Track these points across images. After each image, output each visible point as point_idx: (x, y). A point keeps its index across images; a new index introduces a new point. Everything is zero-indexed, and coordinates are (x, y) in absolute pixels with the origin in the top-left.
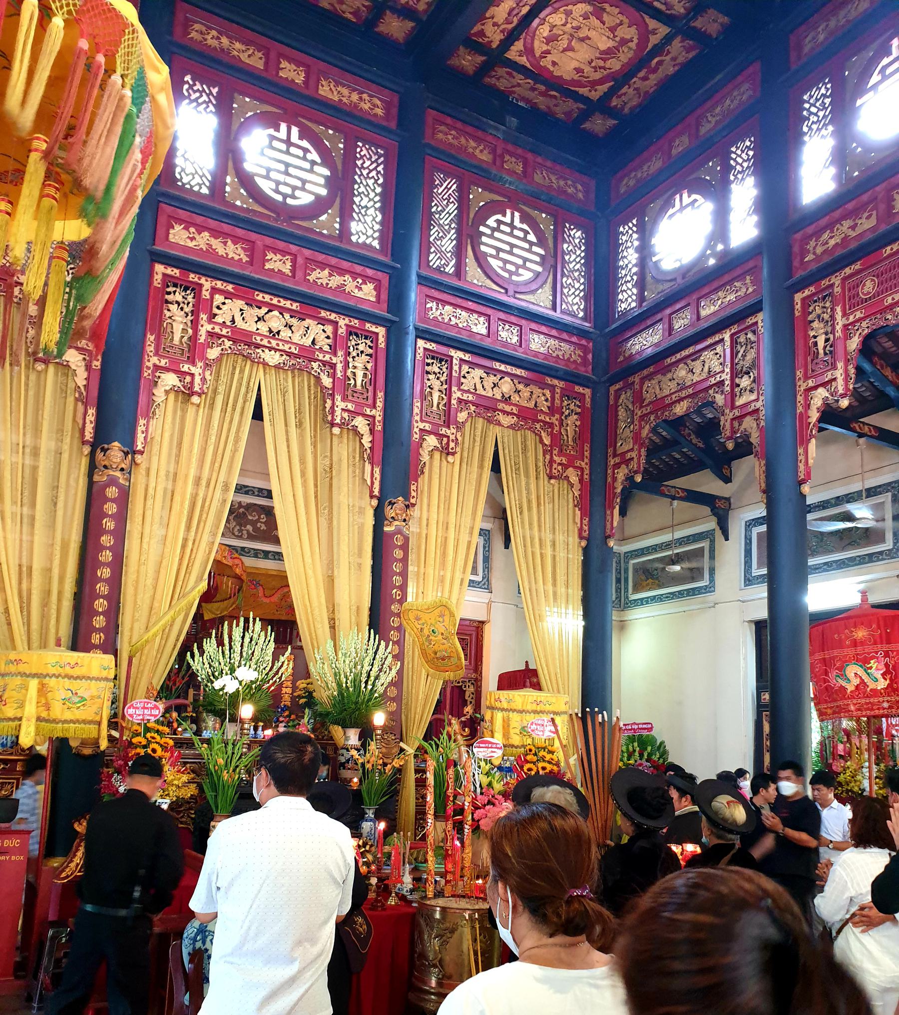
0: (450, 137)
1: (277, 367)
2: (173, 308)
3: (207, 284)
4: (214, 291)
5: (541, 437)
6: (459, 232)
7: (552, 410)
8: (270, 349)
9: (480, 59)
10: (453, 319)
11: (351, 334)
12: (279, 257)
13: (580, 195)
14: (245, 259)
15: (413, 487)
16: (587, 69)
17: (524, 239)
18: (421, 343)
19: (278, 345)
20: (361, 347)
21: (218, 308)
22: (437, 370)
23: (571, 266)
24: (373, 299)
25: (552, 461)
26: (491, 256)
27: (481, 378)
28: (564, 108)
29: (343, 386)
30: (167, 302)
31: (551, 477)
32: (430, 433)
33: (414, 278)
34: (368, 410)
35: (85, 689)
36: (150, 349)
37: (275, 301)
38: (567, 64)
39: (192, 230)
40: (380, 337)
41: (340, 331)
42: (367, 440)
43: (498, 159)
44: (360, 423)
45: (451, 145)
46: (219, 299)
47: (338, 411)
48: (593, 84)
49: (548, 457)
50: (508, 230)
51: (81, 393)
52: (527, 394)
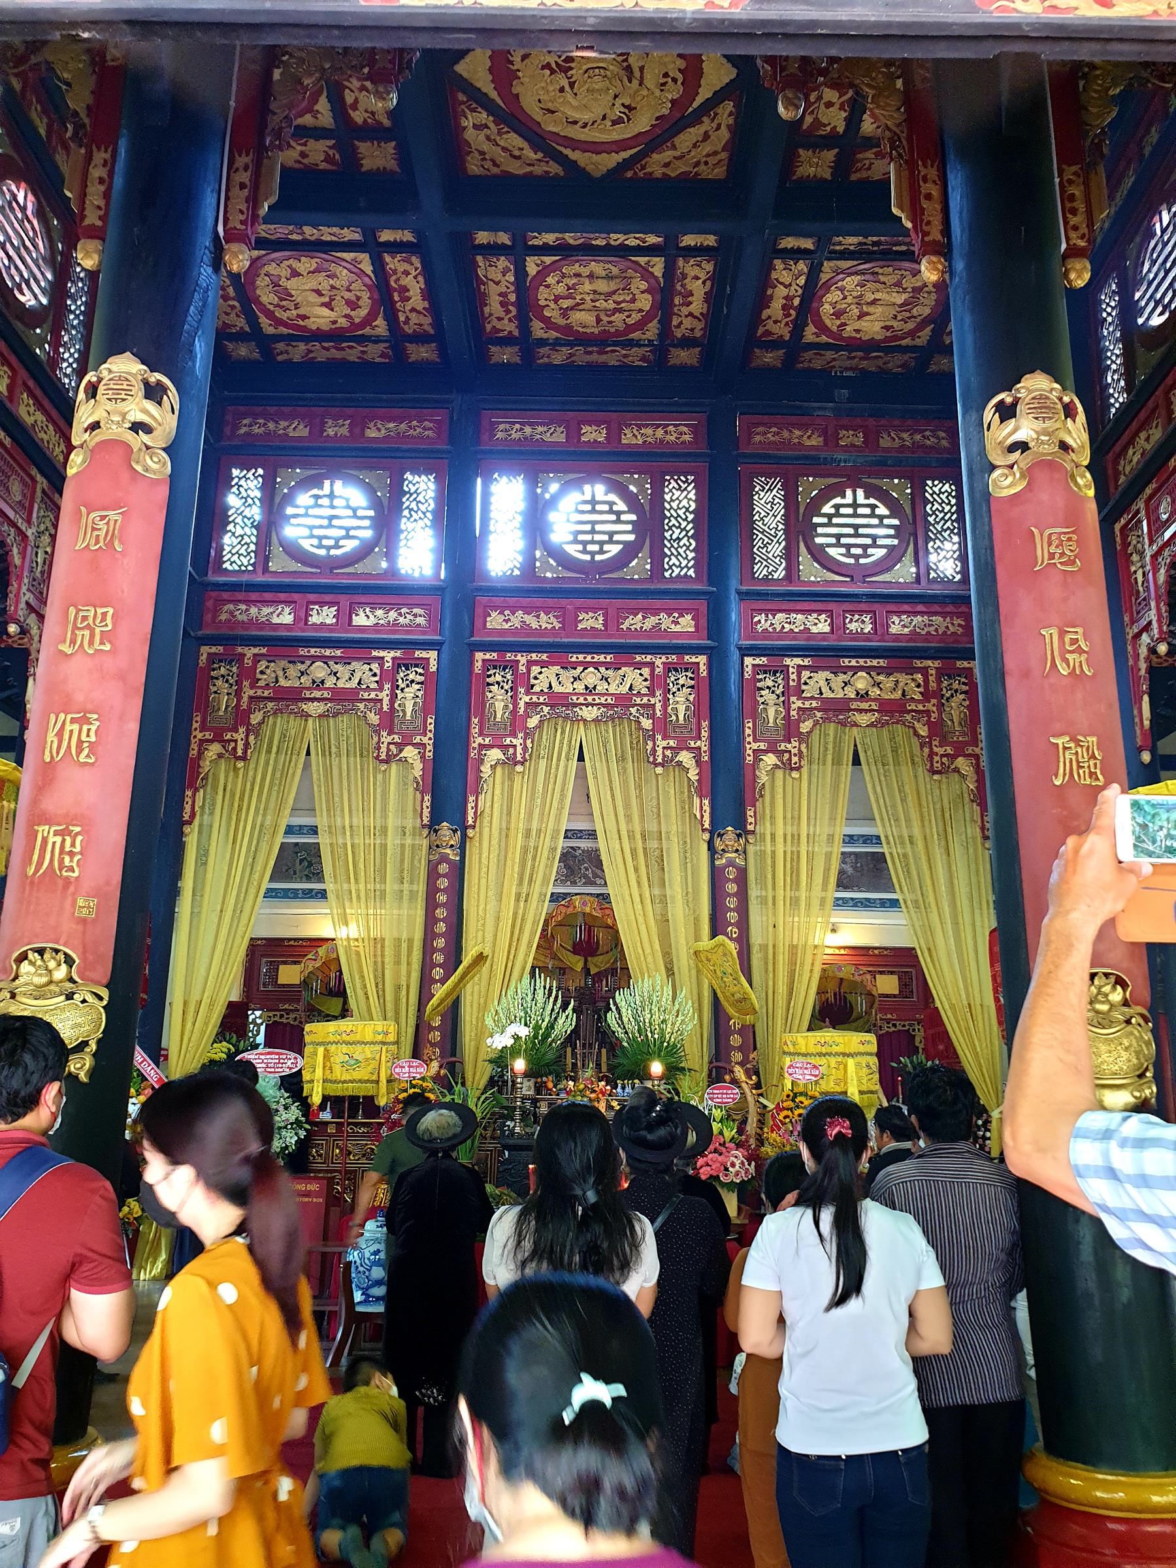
0: (769, 435)
1: (596, 721)
2: (495, 688)
3: (522, 659)
4: (530, 663)
5: (914, 728)
6: (786, 532)
7: (926, 696)
8: (587, 705)
10: (786, 625)
13: (944, 443)
14: (558, 626)
15: (750, 813)
16: (895, 324)
17: (873, 515)
18: (748, 661)
20: (681, 682)
21: (536, 678)
22: (770, 684)
23: (939, 527)
24: (693, 630)
25: (932, 754)
26: (829, 545)
28: (895, 363)
29: (663, 726)
30: (489, 684)
31: (934, 772)
32: (766, 752)
33: (733, 597)
34: (692, 743)
35: (359, 1052)
36: (475, 731)
38: (872, 328)
39: (507, 612)
40: (701, 665)
41: (658, 670)
42: (693, 774)
43: (831, 440)
44: (685, 757)
45: (774, 443)
46: (535, 670)
47: (659, 751)
48: (912, 333)
49: (926, 750)
50: (850, 511)
51: (418, 783)
52: (891, 685)
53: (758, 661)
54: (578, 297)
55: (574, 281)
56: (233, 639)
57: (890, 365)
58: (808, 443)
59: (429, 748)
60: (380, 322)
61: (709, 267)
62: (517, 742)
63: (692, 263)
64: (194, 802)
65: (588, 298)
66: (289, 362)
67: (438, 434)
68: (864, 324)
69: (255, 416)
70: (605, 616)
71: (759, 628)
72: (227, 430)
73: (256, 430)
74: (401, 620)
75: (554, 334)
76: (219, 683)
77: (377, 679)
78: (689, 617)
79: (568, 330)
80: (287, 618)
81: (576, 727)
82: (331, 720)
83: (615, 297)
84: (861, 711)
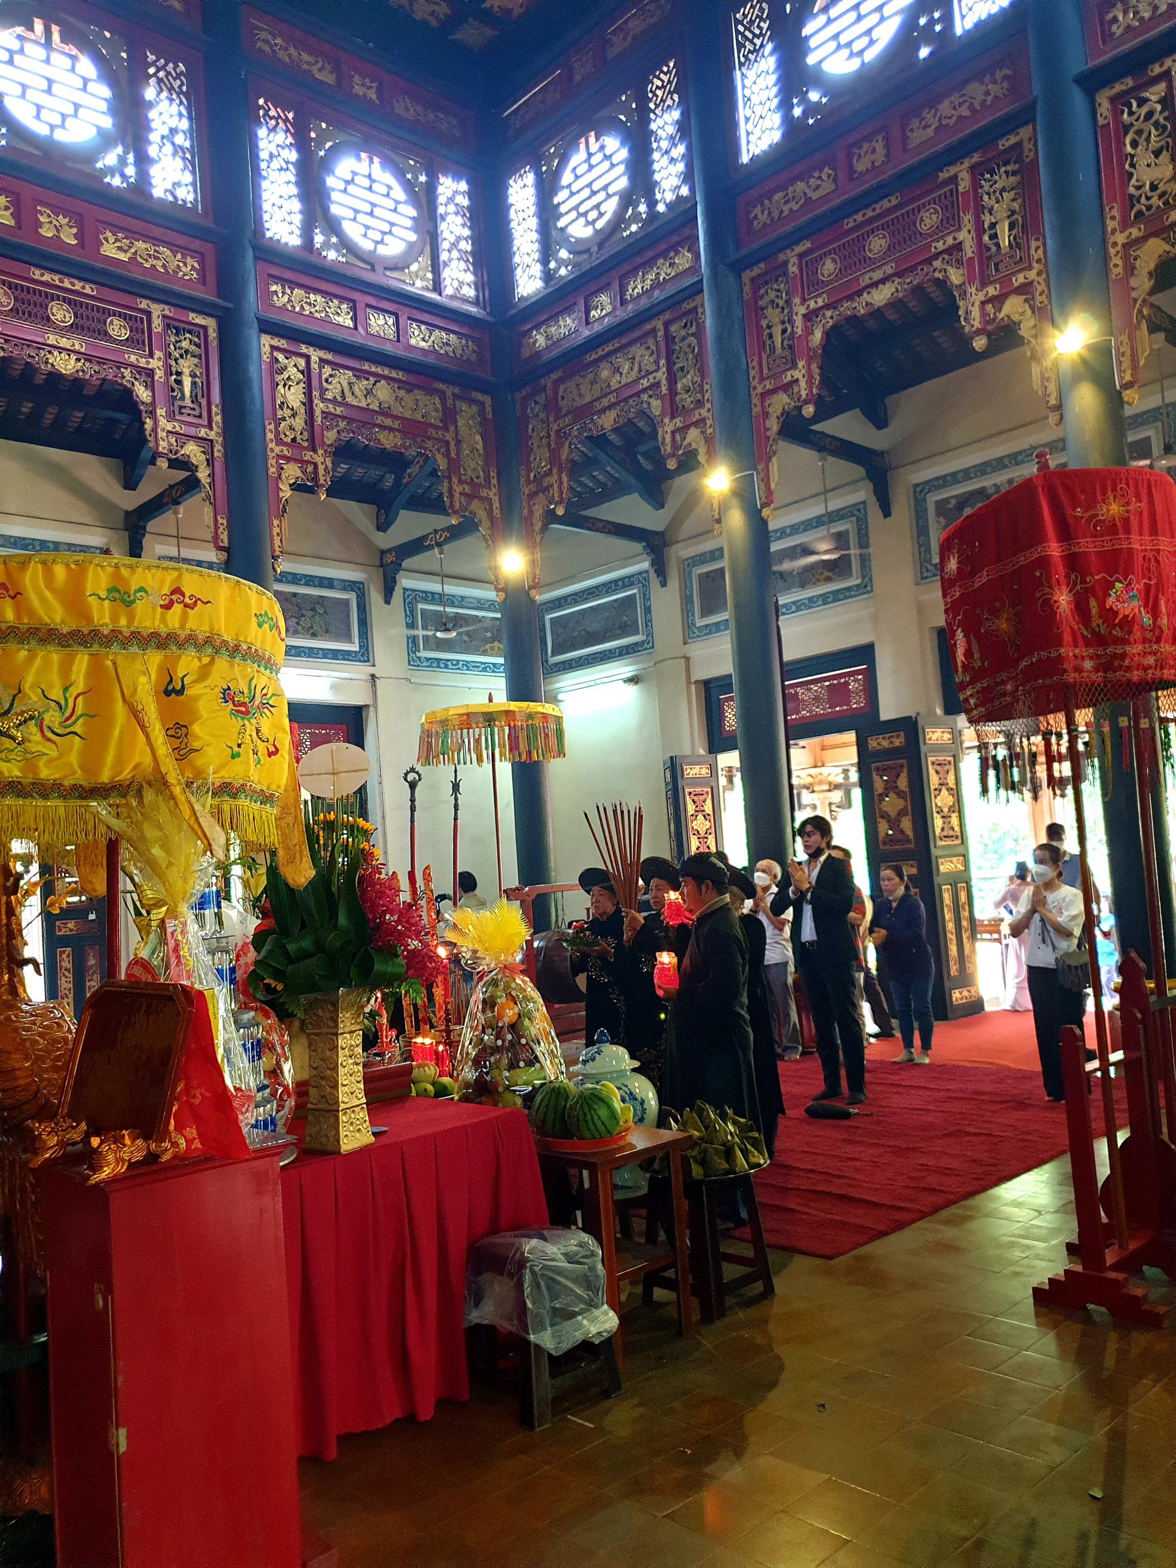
2: (769, 311)
30: (763, 309)
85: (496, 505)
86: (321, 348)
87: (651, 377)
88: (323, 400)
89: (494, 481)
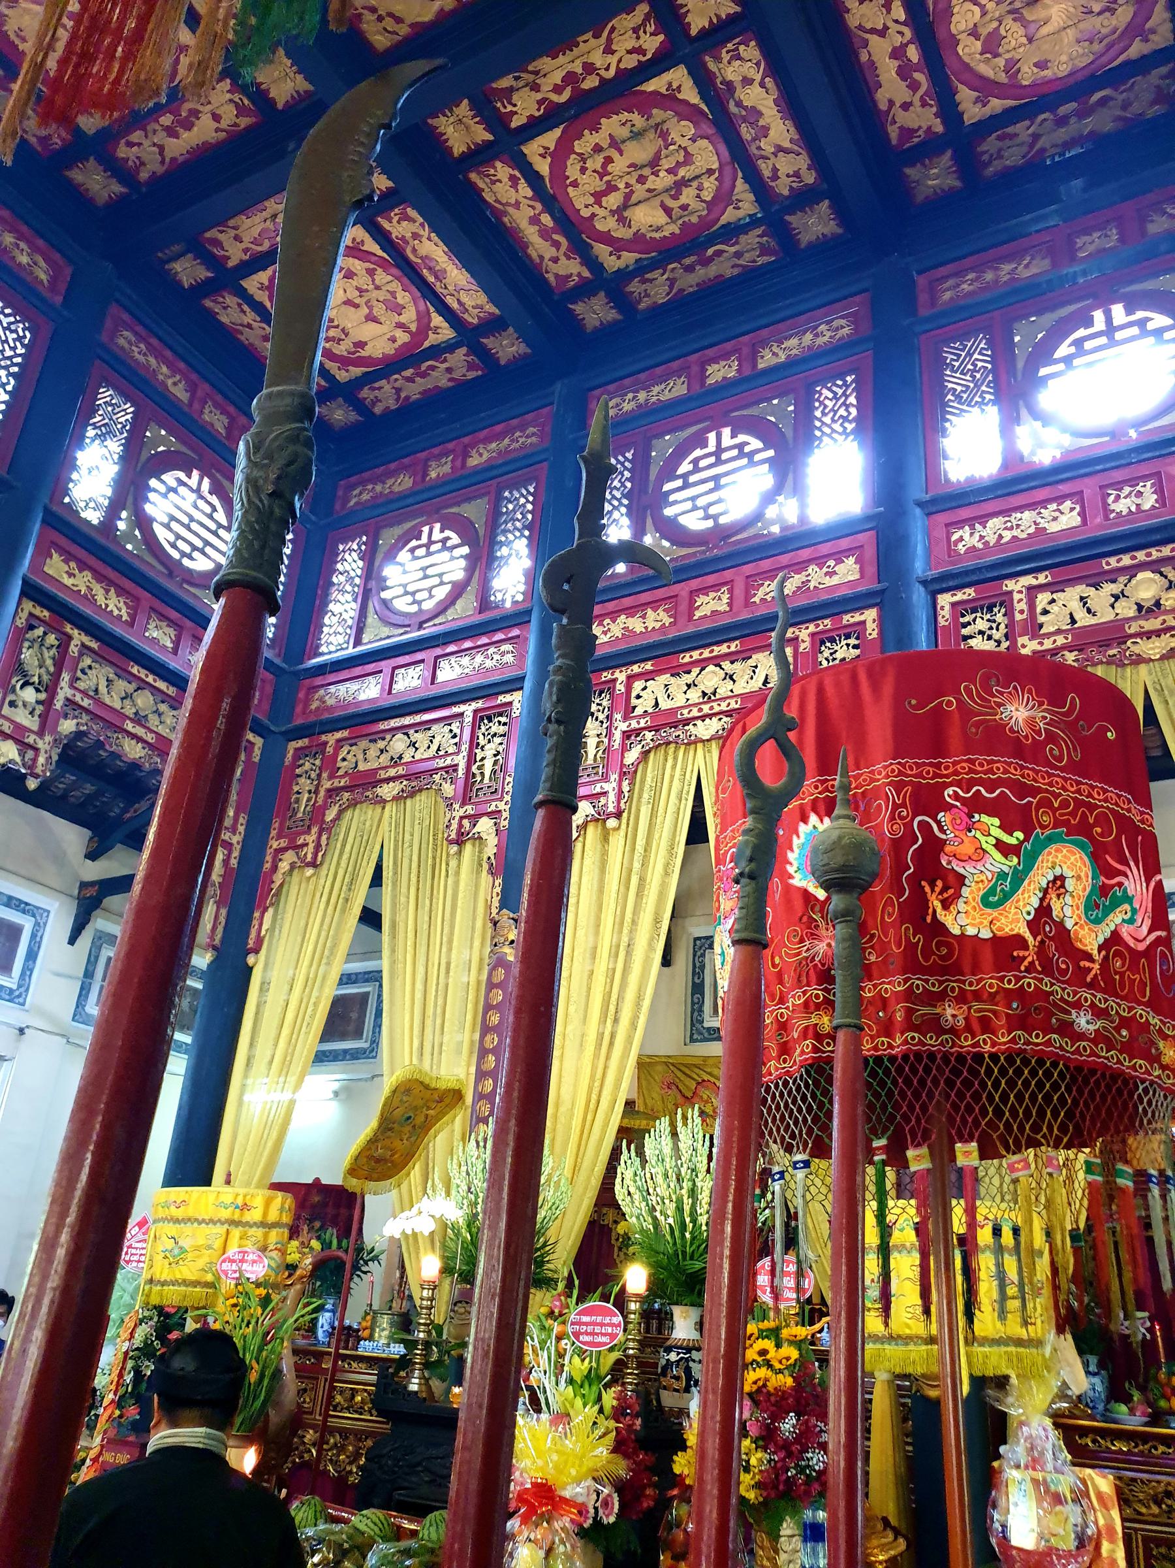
0: (965, 286)
3: (621, 676)
4: (631, 679)
8: (703, 718)
9: (946, 158)
11: (823, 643)
12: (712, 595)
14: (667, 621)
18: (945, 600)
19: (712, 708)
21: (638, 697)
24: (857, 576)
27: (1082, 598)
37: (706, 654)
39: (607, 621)
41: (802, 646)
53: (959, 596)
54: (622, 186)
55: (599, 159)
56: (314, 729)
57: (1136, 108)
58: (1026, 274)
59: (505, 815)
60: (437, 320)
61: (751, 51)
62: (610, 787)
63: (726, 57)
64: (261, 925)
65: (633, 181)
66: (387, 412)
67: (542, 435)
68: (1044, 50)
69: (363, 483)
70: (731, 591)
71: (961, 548)
72: (337, 507)
73: (365, 497)
74: (489, 664)
75: (629, 258)
76: (302, 780)
77: (457, 740)
78: (852, 560)
79: (638, 241)
80: (368, 691)
81: (692, 753)
82: (409, 802)
83: (666, 164)
84: (1148, 635)
85: (236, 854)
86: (88, 633)
87: (449, 759)
88: (72, 686)
89: (241, 829)
